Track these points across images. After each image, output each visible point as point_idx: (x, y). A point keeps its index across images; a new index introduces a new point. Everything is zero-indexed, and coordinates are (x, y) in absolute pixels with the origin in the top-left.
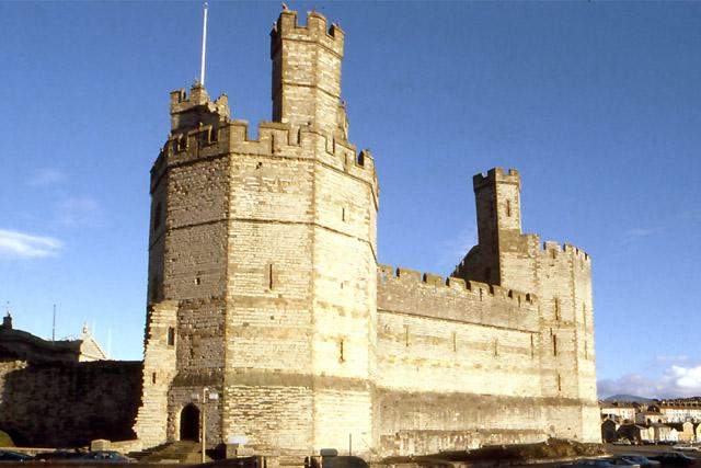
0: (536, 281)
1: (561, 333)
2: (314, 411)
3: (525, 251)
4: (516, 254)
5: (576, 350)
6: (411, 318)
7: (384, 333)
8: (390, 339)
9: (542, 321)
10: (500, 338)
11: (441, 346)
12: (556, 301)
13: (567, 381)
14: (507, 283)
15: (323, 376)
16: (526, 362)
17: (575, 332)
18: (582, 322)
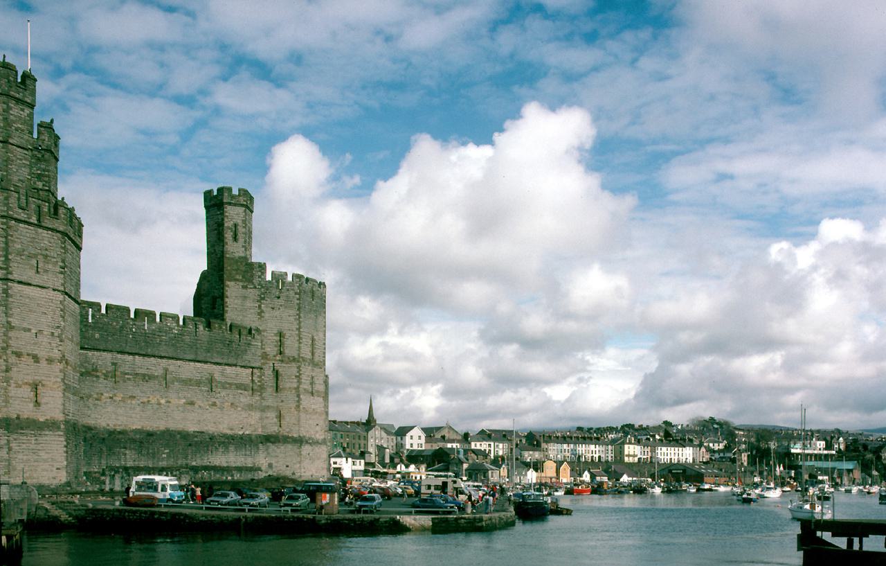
0: (260, 313)
1: (281, 368)
2: (10, 449)
3: (251, 282)
4: (241, 284)
5: (298, 387)
6: (119, 356)
7: (88, 372)
8: (97, 377)
9: (265, 356)
10: (217, 376)
11: (151, 383)
12: (281, 335)
13: (289, 419)
14: (231, 316)
15: (18, 418)
16: (245, 398)
17: (299, 367)
18: (309, 356)
